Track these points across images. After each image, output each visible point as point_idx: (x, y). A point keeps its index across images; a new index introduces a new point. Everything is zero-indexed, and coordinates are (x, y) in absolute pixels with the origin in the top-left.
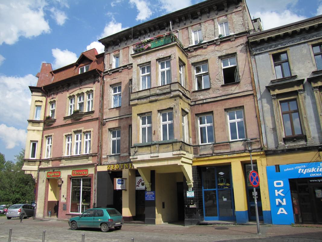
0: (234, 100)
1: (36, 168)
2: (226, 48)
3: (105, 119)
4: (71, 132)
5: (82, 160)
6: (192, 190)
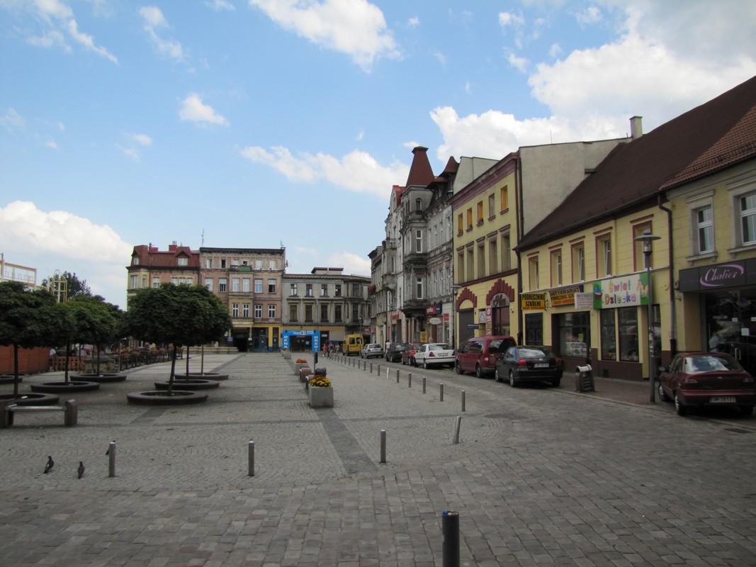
2: (272, 275)
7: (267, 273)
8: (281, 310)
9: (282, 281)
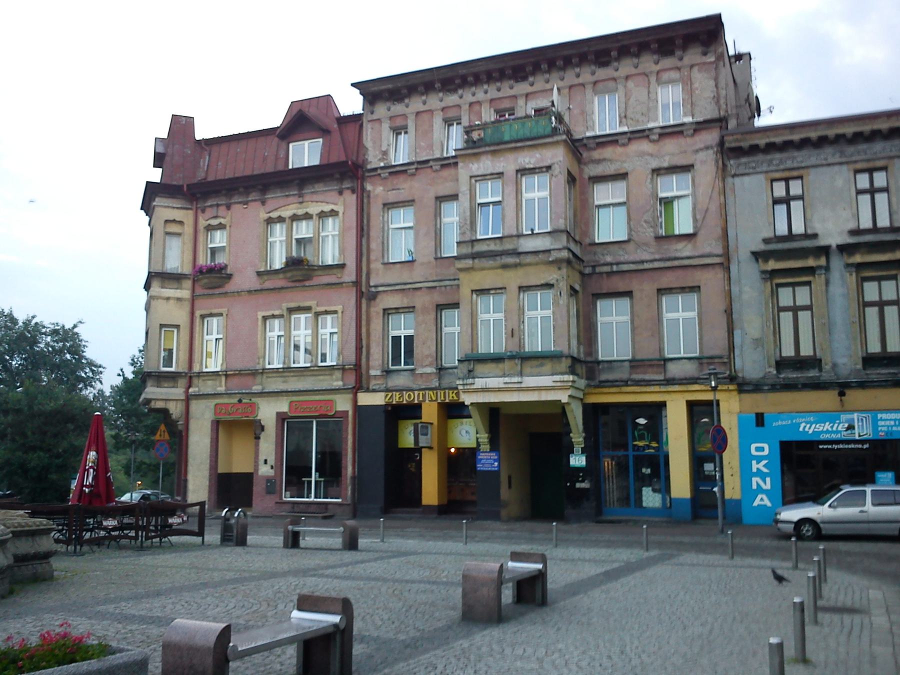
0: (680, 273)
1: (178, 392)
3: (376, 286)
4: (281, 309)
5: (314, 378)
6: (582, 453)
7: (644, 146)
8: (729, 312)
9: (723, 172)
